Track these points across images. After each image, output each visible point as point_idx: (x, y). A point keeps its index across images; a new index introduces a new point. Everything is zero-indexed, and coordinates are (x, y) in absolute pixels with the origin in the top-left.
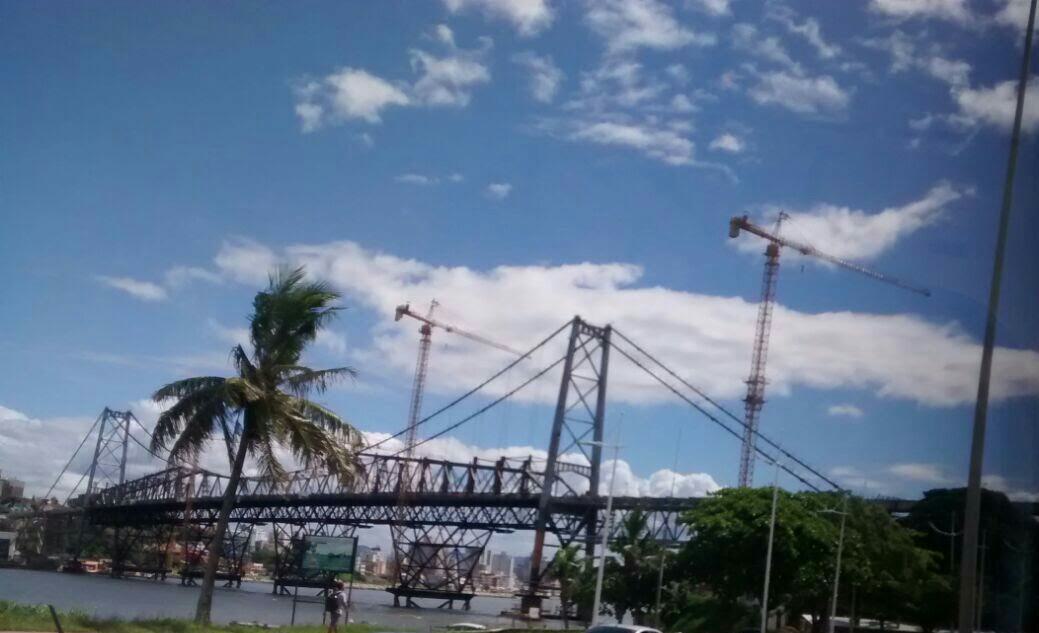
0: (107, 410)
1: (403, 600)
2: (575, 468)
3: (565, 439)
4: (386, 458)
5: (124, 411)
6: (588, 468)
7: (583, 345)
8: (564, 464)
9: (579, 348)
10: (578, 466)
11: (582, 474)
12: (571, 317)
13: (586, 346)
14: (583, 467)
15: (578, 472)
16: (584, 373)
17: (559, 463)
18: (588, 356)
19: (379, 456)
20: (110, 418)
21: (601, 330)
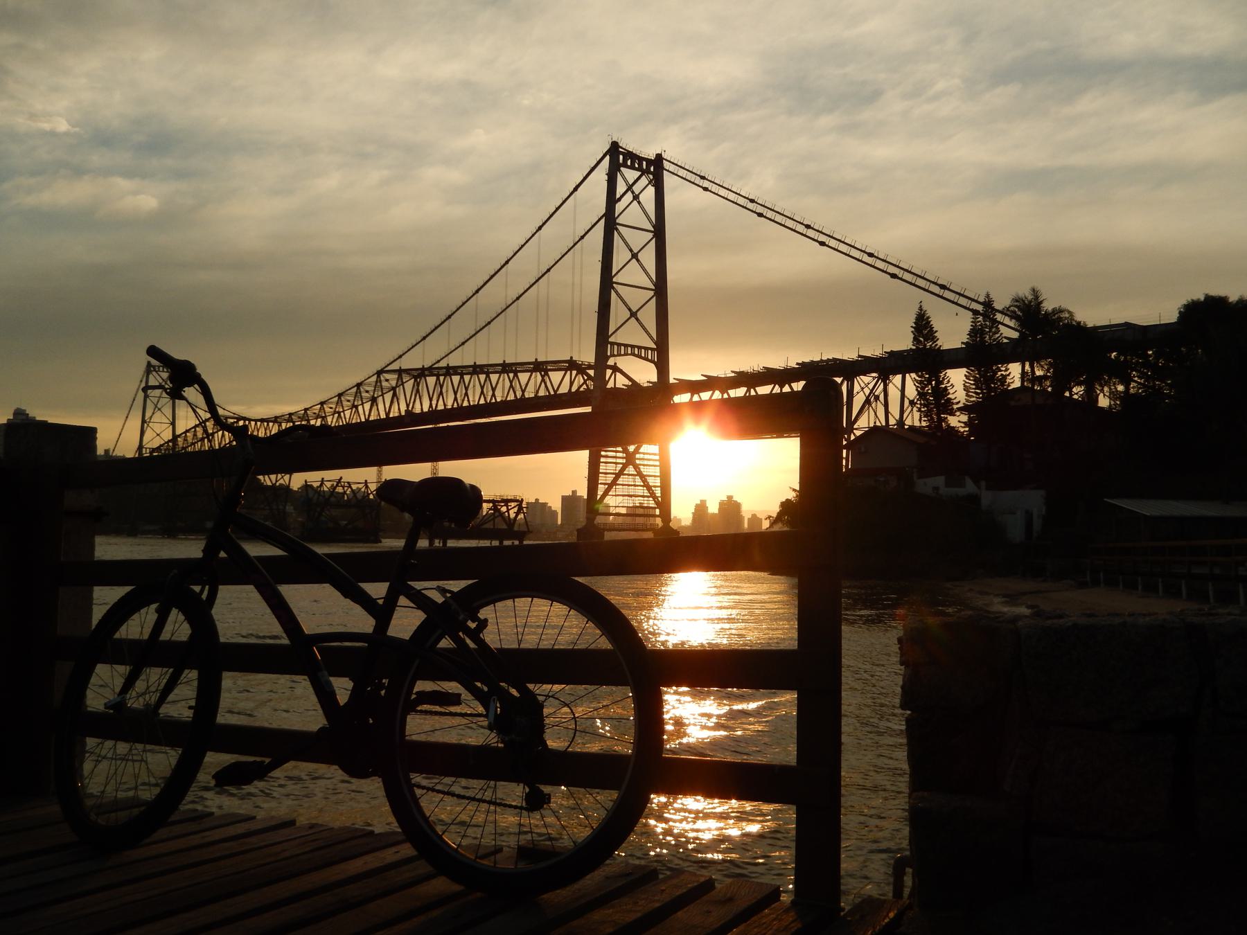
3: (618, 313)
6: (652, 349)
7: (630, 188)
8: (619, 345)
10: (640, 348)
11: (646, 359)
12: (607, 147)
13: (634, 188)
14: (646, 349)
15: (639, 356)
16: (633, 215)
17: (613, 344)
18: (636, 197)
19: (407, 371)
20: (154, 373)
21: (649, 162)
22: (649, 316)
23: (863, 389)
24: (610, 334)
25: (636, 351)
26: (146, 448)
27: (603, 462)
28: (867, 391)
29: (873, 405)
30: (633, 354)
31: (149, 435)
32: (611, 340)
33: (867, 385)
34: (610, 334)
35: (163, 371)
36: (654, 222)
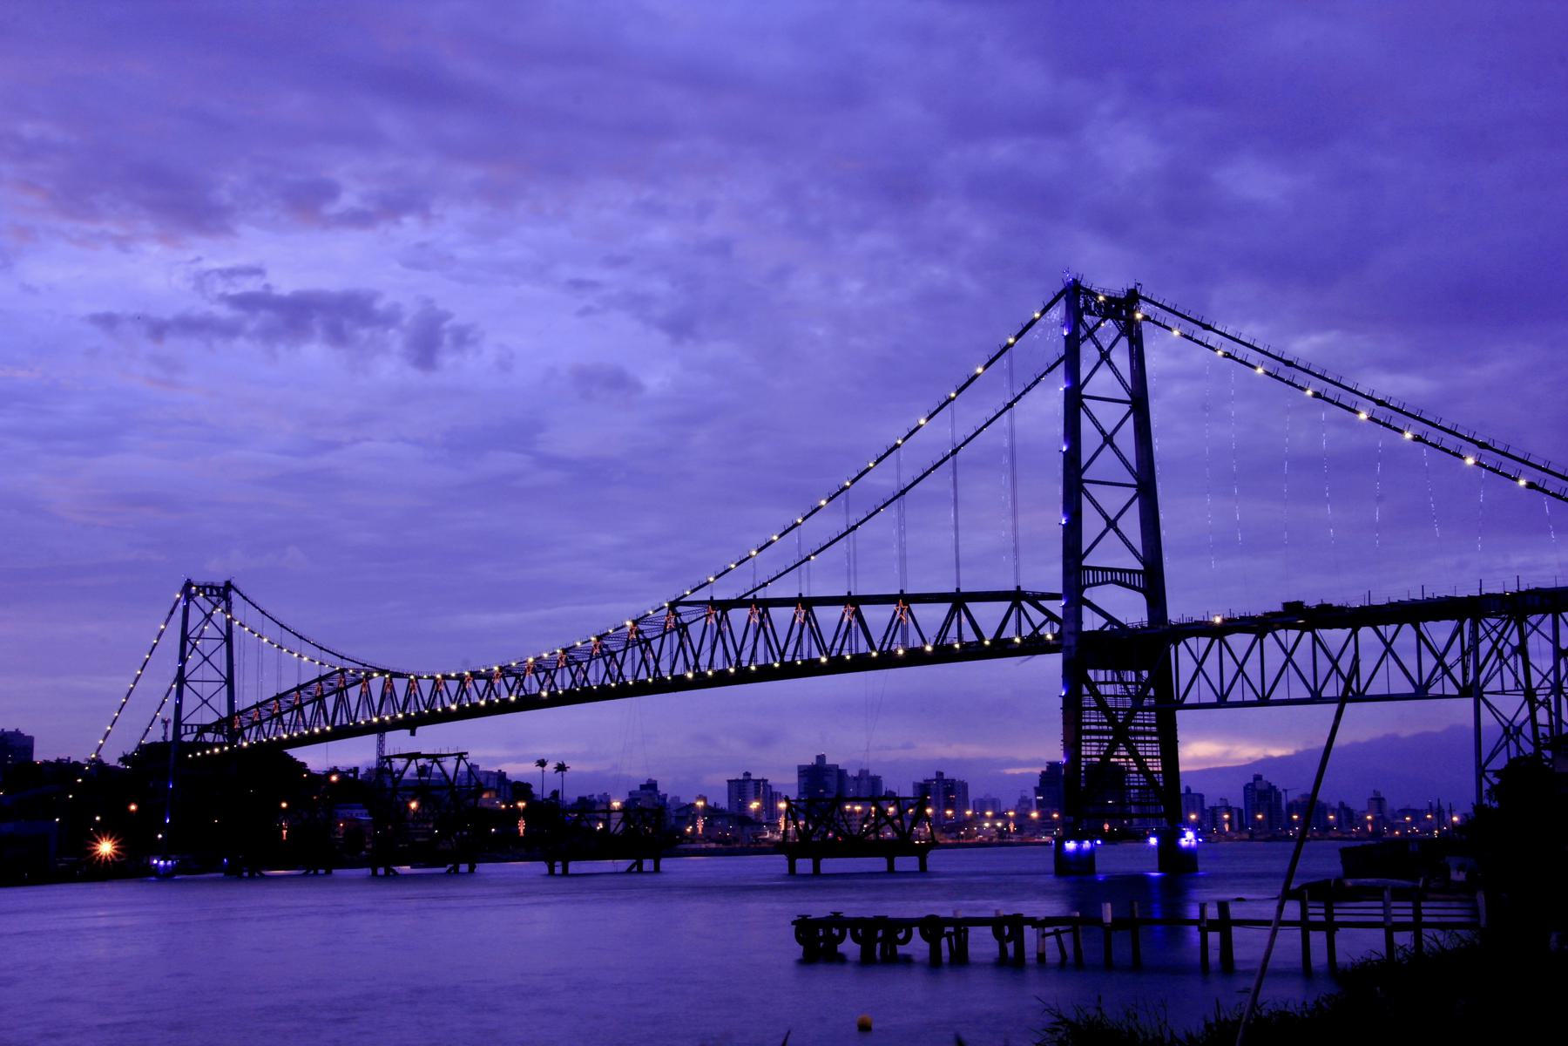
0: (189, 584)
1: (804, 865)
2: (1117, 577)
3: (1092, 524)
4: (725, 605)
5: (220, 581)
6: (1139, 572)
8: (1094, 569)
9: (1084, 339)
18: (1105, 356)
22: (1131, 525)
23: (1488, 634)
24: (1083, 552)
25: (1117, 577)
26: (186, 725)
27: (1086, 741)
28: (1494, 636)
29: (1511, 661)
30: (1116, 582)
31: (190, 701)
32: (1085, 563)
33: (1494, 628)
34: (1083, 552)
35: (211, 595)
36: (1130, 385)
